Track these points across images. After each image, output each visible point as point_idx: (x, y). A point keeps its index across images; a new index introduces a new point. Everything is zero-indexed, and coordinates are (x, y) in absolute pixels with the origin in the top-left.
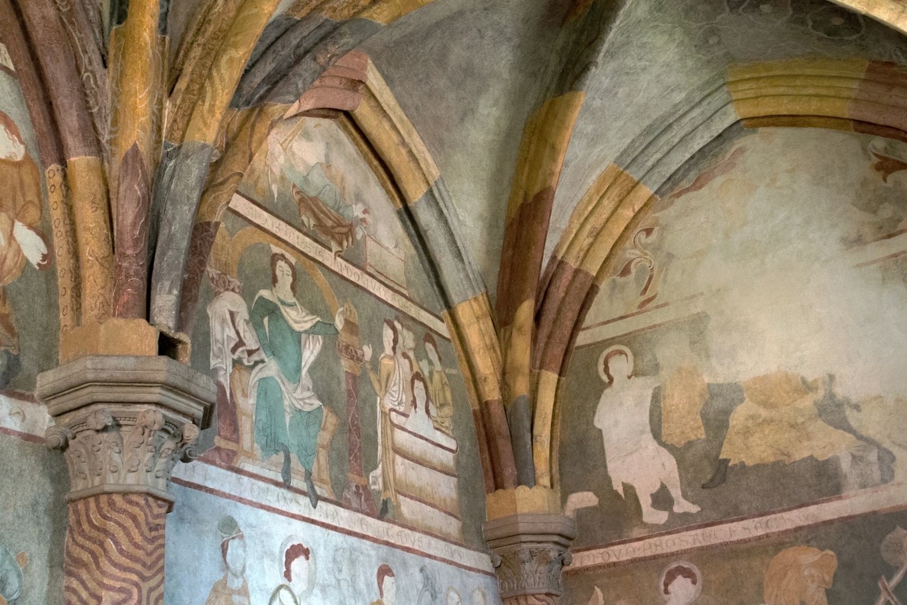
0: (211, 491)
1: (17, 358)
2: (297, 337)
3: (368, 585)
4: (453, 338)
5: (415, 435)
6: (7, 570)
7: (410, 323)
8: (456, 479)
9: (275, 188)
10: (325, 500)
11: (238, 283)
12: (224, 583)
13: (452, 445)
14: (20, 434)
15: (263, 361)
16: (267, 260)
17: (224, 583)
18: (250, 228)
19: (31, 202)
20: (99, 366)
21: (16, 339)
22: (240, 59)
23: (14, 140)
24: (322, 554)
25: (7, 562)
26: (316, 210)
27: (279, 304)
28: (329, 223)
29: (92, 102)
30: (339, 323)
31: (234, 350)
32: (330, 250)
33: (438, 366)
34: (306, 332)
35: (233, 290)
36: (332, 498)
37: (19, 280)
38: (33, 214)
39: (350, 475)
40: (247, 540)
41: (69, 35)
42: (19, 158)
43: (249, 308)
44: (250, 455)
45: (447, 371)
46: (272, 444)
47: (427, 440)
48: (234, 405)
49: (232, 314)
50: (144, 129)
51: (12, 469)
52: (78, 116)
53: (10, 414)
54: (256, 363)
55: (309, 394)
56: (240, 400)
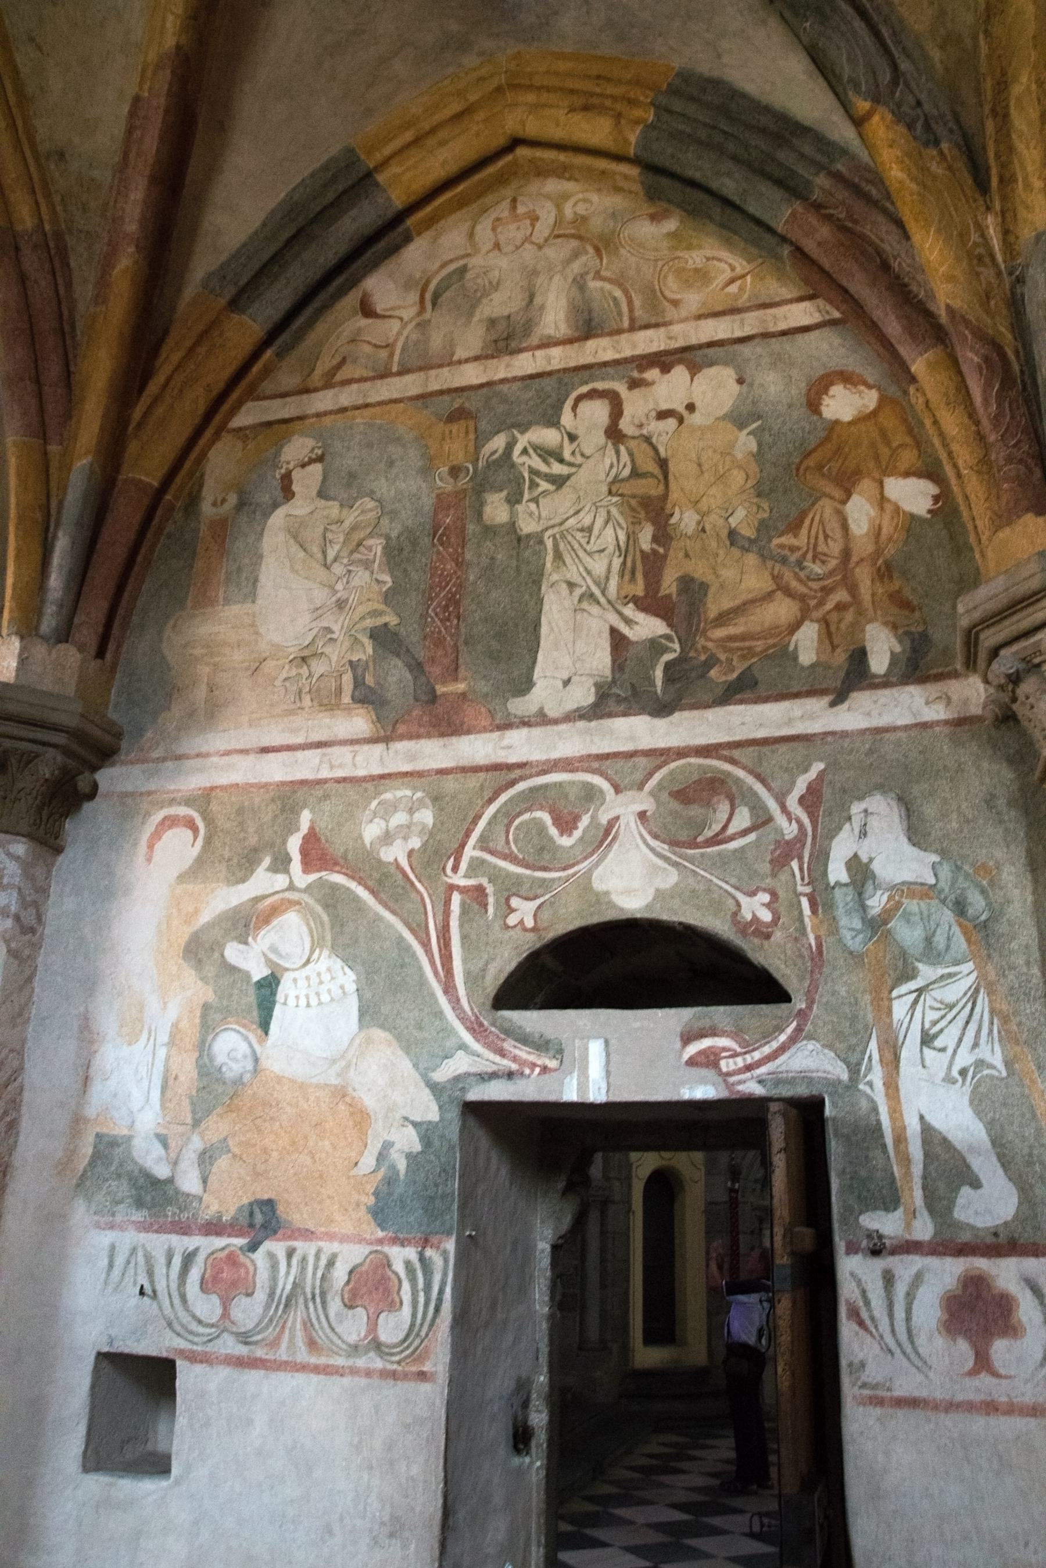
6: (963, 889)
14: (946, 722)
19: (901, 446)
20: (971, 605)
21: (917, 613)
22: (1028, 88)
23: (860, 393)
25: (961, 879)
29: (914, 288)
37: (906, 542)
38: (908, 457)
41: (863, 237)
50: (950, 278)
51: (945, 767)
52: (897, 317)
53: (927, 703)
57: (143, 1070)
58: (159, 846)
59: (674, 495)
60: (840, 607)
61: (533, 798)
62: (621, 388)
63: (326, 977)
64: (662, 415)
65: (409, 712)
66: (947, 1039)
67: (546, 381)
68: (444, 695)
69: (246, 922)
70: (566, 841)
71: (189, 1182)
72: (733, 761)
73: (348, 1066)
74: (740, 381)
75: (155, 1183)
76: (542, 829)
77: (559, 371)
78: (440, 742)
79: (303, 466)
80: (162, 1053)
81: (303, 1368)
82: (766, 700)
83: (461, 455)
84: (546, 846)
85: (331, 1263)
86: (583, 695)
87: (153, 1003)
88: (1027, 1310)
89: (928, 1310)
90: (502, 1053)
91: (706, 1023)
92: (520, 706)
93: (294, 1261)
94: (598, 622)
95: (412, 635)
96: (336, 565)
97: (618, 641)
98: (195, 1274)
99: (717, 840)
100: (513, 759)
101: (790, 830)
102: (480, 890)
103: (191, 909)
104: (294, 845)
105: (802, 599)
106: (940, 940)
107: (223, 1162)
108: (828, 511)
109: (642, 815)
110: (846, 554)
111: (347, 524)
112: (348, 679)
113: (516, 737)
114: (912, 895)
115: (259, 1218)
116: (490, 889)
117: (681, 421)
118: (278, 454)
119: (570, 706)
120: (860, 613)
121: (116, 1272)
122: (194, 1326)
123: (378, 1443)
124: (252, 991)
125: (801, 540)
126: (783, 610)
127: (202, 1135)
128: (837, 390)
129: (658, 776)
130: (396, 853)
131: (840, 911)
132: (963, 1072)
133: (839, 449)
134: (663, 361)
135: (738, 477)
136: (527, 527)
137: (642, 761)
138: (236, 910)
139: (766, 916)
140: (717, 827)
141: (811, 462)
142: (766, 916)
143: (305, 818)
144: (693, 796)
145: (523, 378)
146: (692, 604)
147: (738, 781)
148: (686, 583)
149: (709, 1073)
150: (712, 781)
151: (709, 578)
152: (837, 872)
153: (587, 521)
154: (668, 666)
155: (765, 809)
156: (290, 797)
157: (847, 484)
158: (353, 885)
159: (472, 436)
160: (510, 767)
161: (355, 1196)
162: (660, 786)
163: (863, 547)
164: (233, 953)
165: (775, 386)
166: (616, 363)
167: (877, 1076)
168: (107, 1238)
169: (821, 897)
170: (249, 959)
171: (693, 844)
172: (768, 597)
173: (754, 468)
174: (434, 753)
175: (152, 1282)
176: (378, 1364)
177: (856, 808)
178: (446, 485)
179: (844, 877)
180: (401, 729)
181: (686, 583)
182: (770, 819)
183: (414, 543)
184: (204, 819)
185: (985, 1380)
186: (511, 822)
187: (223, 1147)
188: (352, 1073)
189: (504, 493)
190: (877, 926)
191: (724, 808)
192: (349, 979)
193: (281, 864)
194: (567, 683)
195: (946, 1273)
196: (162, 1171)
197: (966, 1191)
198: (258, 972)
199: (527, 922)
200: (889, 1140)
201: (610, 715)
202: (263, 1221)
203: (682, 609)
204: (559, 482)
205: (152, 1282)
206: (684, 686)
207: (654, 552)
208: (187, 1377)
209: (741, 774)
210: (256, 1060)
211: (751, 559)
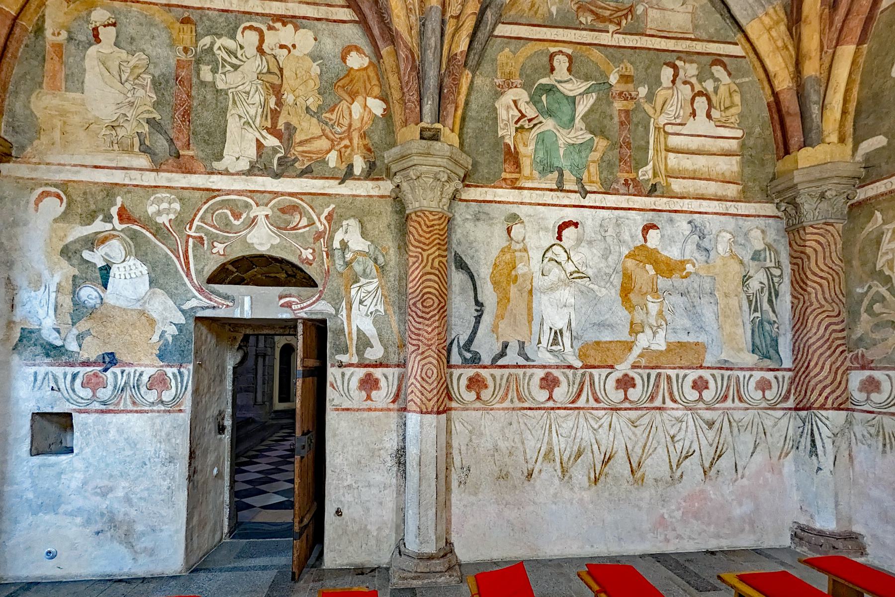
0: (499, 202)
1: (374, 163)
2: (573, 101)
3: (632, 237)
4: (747, 53)
5: (692, 135)
7: (695, 57)
8: (739, 158)
9: (554, 10)
10: (594, 192)
11: (520, 81)
12: (509, 247)
13: (739, 133)
15: (541, 123)
16: (546, 59)
17: (509, 247)
18: (530, 44)
24: (589, 223)
26: (594, 9)
27: (556, 84)
28: (607, 13)
30: (613, 79)
31: (516, 123)
32: (608, 32)
33: (725, 79)
34: (580, 94)
35: (516, 87)
36: (603, 190)
38: (377, 91)
39: (619, 174)
40: (526, 223)
43: (529, 94)
44: (530, 178)
45: (737, 81)
46: (546, 168)
47: (705, 136)
48: (517, 153)
49: (515, 102)
54: (535, 125)
55: (582, 132)
56: (521, 149)
57: (44, 302)
58: (41, 205)
59: (285, 86)
60: (346, 147)
62: (264, 28)
63: (133, 267)
64: (282, 47)
65: (167, 160)
66: (367, 303)
67: (230, 15)
68: (183, 155)
69: (92, 242)
70: (236, 223)
71: (73, 346)
72: (302, 200)
73: (145, 303)
74: (316, 39)
75: (56, 347)
76: (227, 217)
77: (235, 11)
78: (182, 175)
79: (105, 26)
80: (53, 295)
81: (131, 411)
82: (316, 178)
83: (189, 42)
84: (228, 224)
85: (141, 375)
86: (244, 165)
87: (46, 274)
88: (383, 383)
89: (354, 383)
90: (210, 300)
91: (288, 292)
92: (216, 165)
93: (125, 374)
94: (252, 135)
95: (167, 124)
96: (126, 84)
97: (259, 145)
98: (78, 381)
99: (293, 229)
100: (214, 187)
101: (321, 228)
102: (201, 238)
103: (62, 234)
104: (114, 211)
105: (332, 141)
106: (368, 271)
107: (88, 339)
108: (345, 106)
109: (267, 216)
110: (350, 126)
111: (132, 63)
112: (136, 140)
114: (361, 255)
115: (107, 360)
116: (205, 238)
117: (289, 52)
118: (89, 15)
119: (238, 169)
120: (352, 150)
121: (39, 383)
122: (80, 400)
123: (163, 434)
124: (97, 271)
125: (334, 117)
126: (324, 144)
127: (77, 328)
128: (353, 53)
129: (273, 202)
130: (163, 219)
131: (336, 258)
132: (371, 313)
133: (351, 81)
134: (283, 19)
135: (312, 83)
136: (220, 86)
137: (268, 195)
138: (87, 237)
139: (311, 257)
140: (295, 224)
141: (340, 84)
142: (311, 257)
143: (119, 200)
144: (287, 212)
145: (219, 10)
146: (290, 135)
147: (303, 208)
148: (288, 125)
149: (288, 309)
150: (294, 206)
152: (336, 244)
153: (247, 89)
154: (279, 159)
155: (312, 219)
156: (110, 190)
157: (353, 96)
158: (144, 231)
159: (194, 34)
160: (213, 190)
161: (150, 351)
162: (274, 206)
163: (356, 124)
164: (86, 255)
165: (330, 46)
166: (263, 15)
167: (344, 313)
168: (33, 369)
169: (330, 254)
170: (97, 258)
171: (285, 229)
172: (319, 137)
173: (318, 81)
174: (181, 180)
175: (57, 385)
176: (163, 408)
177: (345, 223)
178: (183, 57)
179: (339, 247)
180: (164, 167)
181: (288, 125)
182: (314, 223)
183: (167, 81)
184: (65, 194)
185: (369, 402)
186: (213, 213)
187: (88, 332)
188: (147, 305)
189: (210, 67)
190: (348, 264)
191: (298, 217)
192: (144, 269)
193: (108, 219)
194: (238, 159)
195: (361, 372)
196: (58, 343)
197: (369, 348)
198: (101, 263)
199: (220, 253)
200: (347, 333)
202: (110, 360)
203: (286, 136)
204: (236, 67)
205: (57, 385)
206: (286, 168)
207: (276, 110)
208: (77, 419)
209: (305, 205)
210: (102, 299)
211: (314, 120)
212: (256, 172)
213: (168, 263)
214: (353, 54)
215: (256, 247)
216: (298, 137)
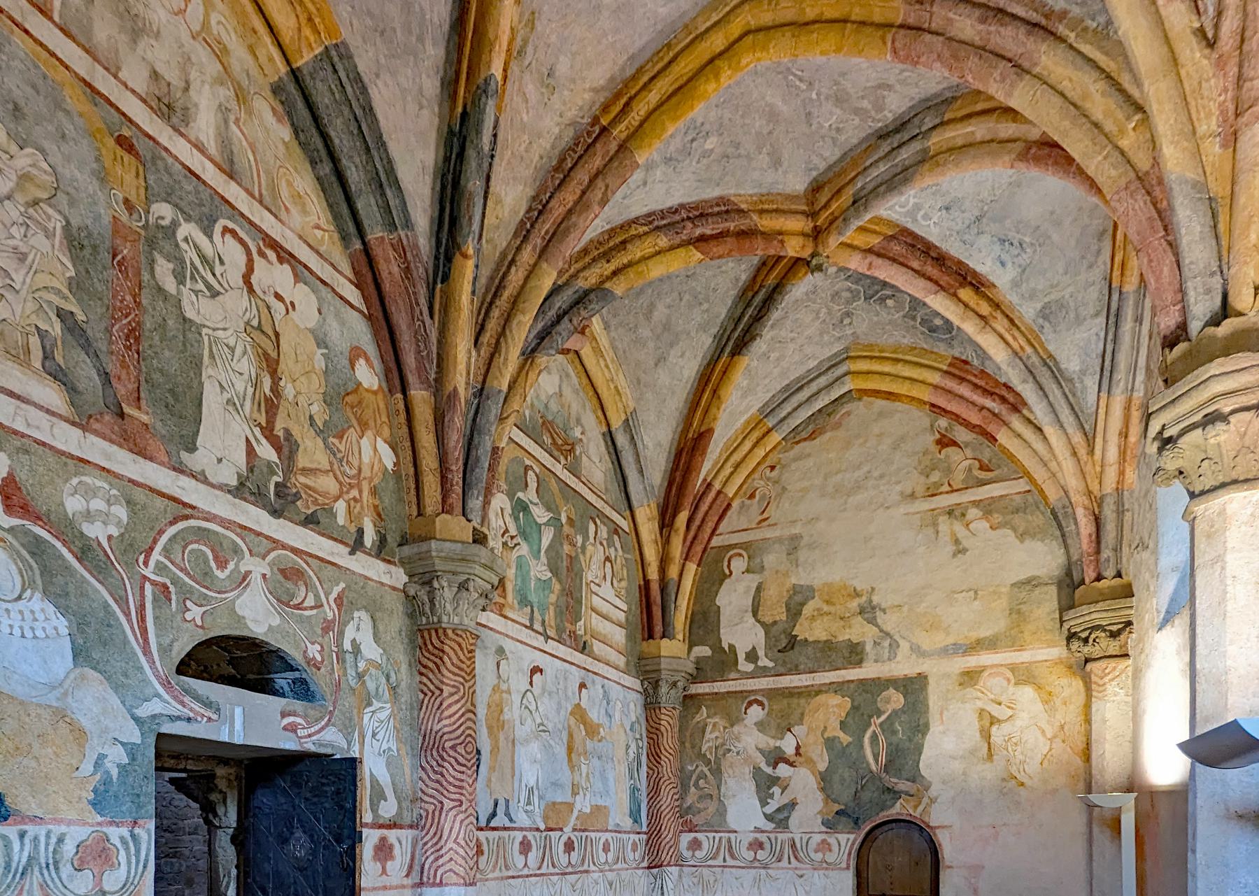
42: (375, 388)
61: (202, 535)
113: (185, 481)
151: (299, 441)
171: (288, 605)
186: (185, 547)
201: (245, 500)
211: (319, 441)
212: (247, 495)
213: (108, 621)
214: (362, 361)
215: (251, 625)
216: (302, 461)
